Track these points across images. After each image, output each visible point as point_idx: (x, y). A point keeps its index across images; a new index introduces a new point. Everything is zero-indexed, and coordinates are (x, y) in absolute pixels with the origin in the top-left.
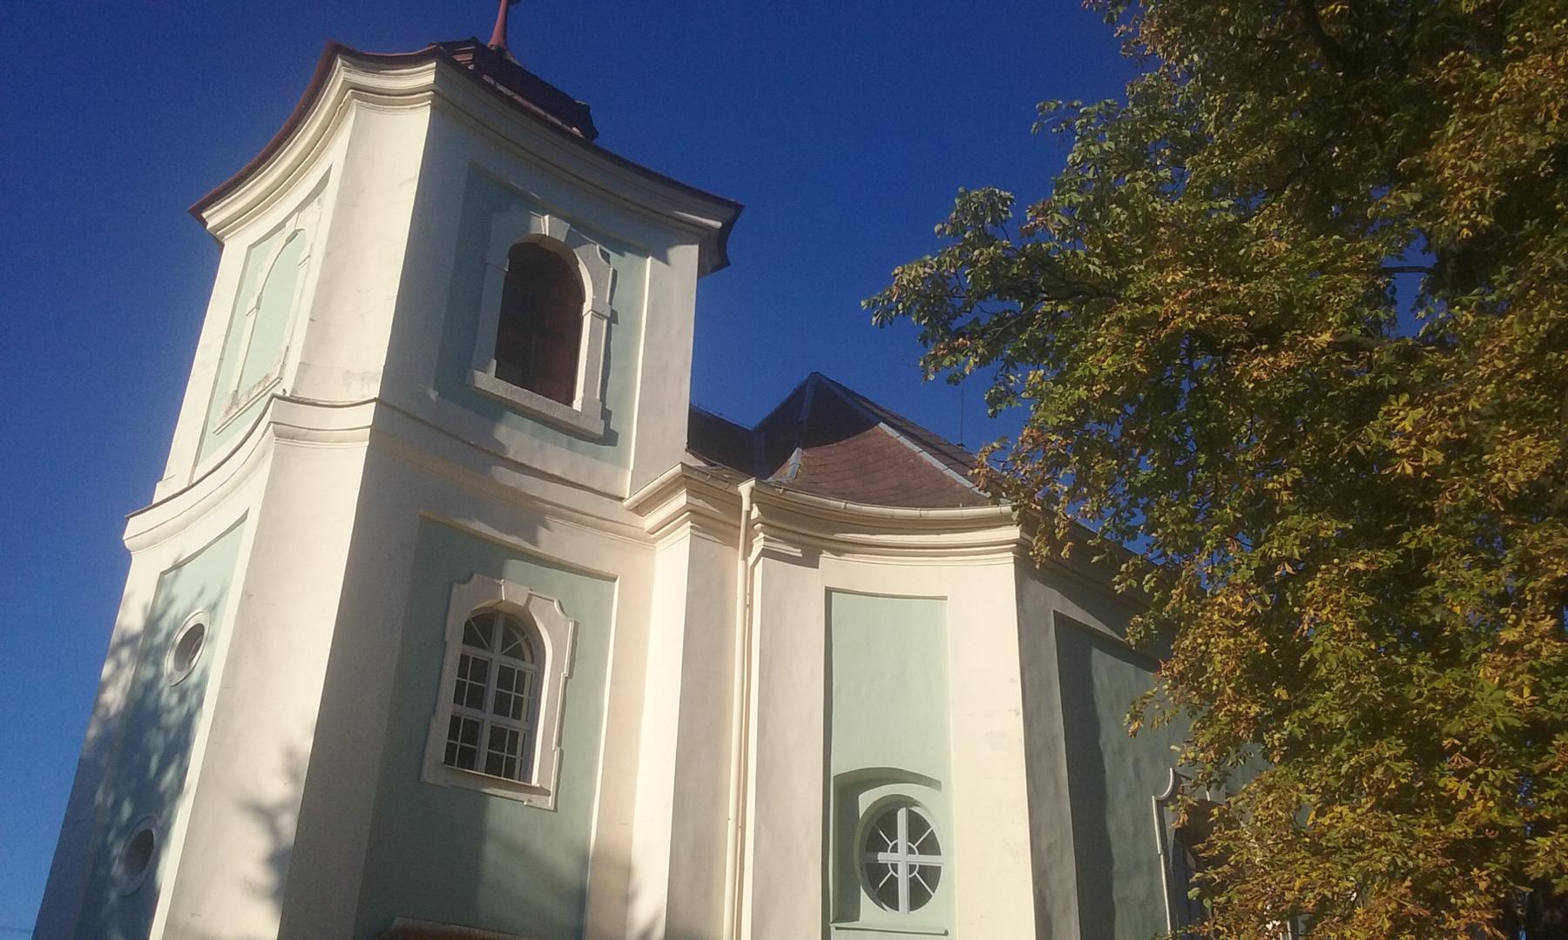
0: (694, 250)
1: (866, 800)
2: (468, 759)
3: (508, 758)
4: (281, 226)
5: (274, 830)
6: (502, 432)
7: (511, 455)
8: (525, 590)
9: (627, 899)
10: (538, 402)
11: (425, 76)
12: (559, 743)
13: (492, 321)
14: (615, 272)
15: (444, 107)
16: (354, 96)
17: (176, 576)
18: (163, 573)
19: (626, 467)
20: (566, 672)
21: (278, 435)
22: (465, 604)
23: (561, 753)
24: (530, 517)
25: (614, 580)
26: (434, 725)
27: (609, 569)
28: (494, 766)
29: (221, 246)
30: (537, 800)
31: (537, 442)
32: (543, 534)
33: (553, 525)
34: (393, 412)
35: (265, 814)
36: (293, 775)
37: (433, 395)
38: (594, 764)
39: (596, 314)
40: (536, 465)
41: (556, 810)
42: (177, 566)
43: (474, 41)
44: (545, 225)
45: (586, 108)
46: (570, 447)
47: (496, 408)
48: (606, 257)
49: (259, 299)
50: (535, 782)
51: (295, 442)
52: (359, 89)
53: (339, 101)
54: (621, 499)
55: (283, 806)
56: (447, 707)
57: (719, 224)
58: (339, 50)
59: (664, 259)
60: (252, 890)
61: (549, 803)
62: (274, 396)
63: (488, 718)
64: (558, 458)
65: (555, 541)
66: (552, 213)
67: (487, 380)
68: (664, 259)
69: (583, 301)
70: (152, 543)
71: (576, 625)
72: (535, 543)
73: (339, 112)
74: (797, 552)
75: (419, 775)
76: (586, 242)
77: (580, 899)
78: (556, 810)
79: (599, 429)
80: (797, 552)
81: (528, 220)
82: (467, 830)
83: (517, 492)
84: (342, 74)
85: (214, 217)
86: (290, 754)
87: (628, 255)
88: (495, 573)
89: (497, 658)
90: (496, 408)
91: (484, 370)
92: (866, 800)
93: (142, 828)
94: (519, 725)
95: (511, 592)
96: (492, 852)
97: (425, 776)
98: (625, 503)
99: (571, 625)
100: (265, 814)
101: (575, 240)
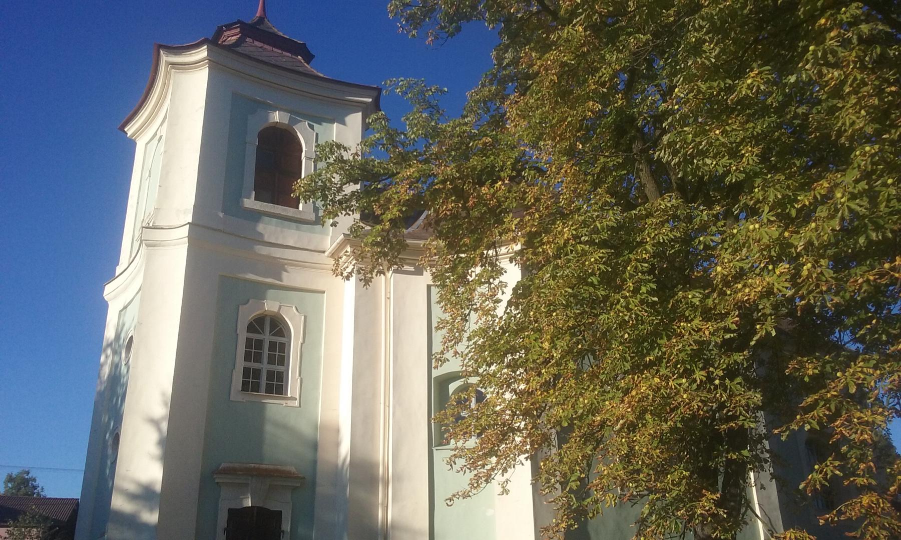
0: (359, 116)
2: (256, 388)
3: (277, 385)
4: (155, 134)
5: (159, 430)
6: (261, 227)
7: (266, 239)
8: (277, 304)
9: (338, 444)
11: (202, 53)
12: (300, 375)
13: (256, 170)
14: (317, 134)
15: (215, 65)
18: (121, 311)
19: (328, 235)
20: (301, 340)
21: (146, 245)
22: (247, 314)
24: (277, 268)
27: (320, 288)
28: (269, 390)
30: (290, 403)
31: (279, 229)
32: (285, 274)
33: (289, 270)
34: (201, 230)
35: (155, 423)
36: (166, 404)
37: (221, 215)
40: (280, 242)
42: (125, 308)
43: (239, 22)
44: (277, 117)
46: (298, 229)
48: (312, 127)
50: (289, 395)
51: (156, 248)
52: (173, 64)
54: (324, 252)
55: (163, 418)
56: (241, 364)
58: (161, 46)
61: (297, 403)
63: (265, 367)
64: (291, 236)
65: (291, 278)
66: (280, 110)
67: (250, 203)
70: (115, 297)
71: (305, 317)
72: (281, 281)
73: (168, 75)
74: (412, 269)
76: (300, 121)
77: (315, 446)
79: (312, 217)
82: (256, 421)
85: (130, 130)
86: (163, 394)
87: (324, 124)
89: (267, 337)
90: (256, 216)
91: (249, 198)
92: (453, 387)
94: (281, 368)
95: (270, 306)
96: (269, 428)
97: (232, 399)
98: (326, 254)
99: (303, 318)
100: (155, 423)
101: (293, 122)
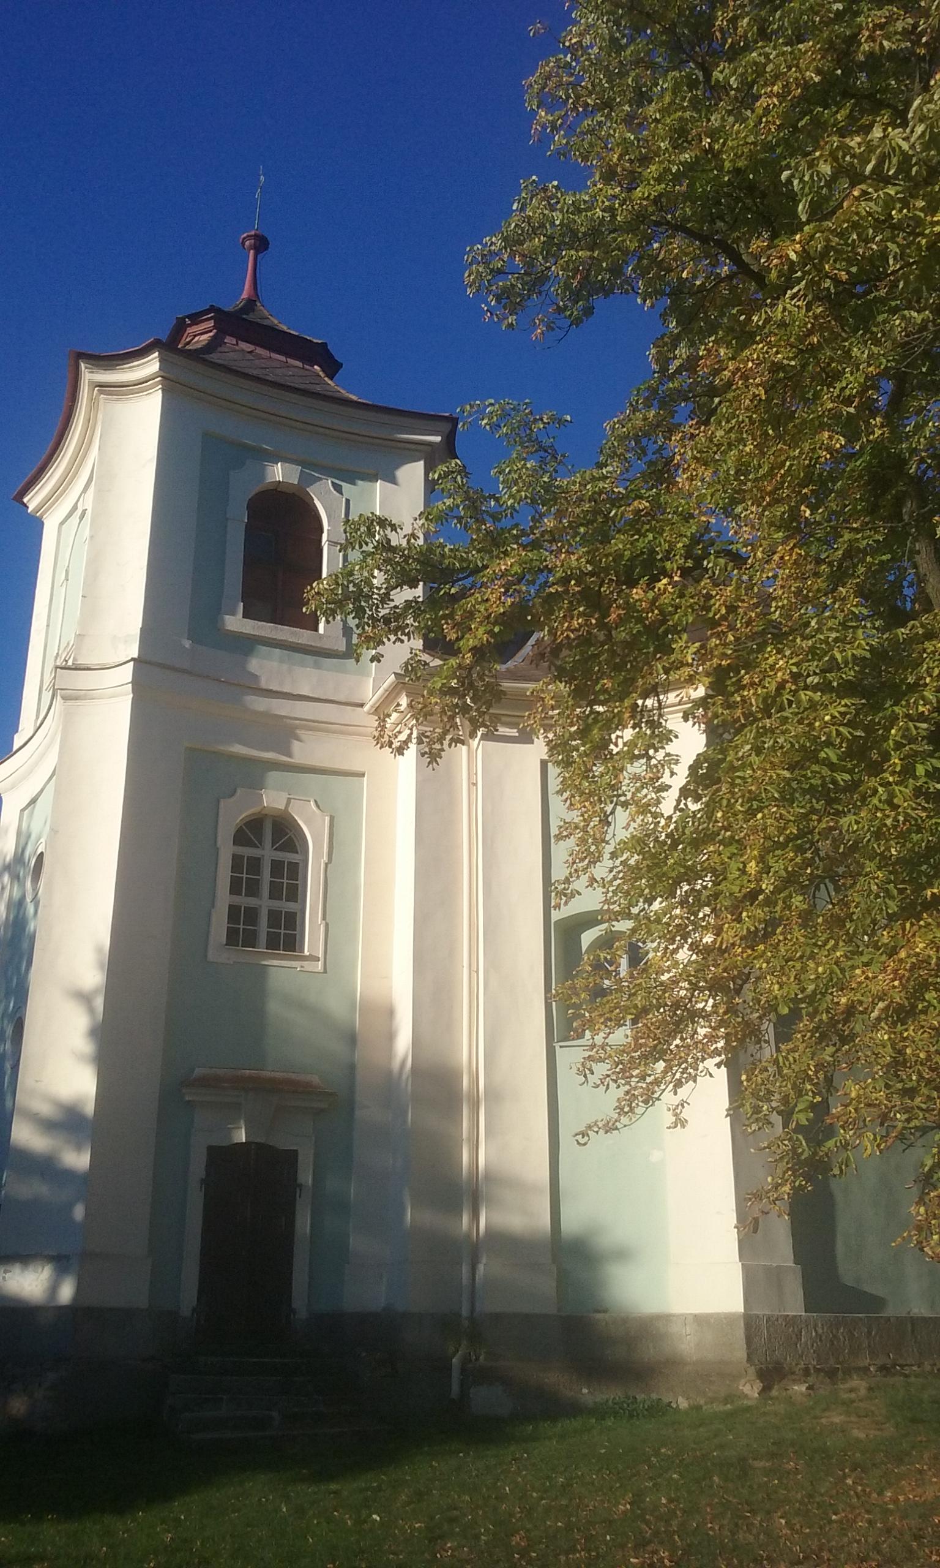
0: (420, 465)
1: (588, 938)
2: (250, 940)
3: (286, 935)
4: (75, 508)
5: (91, 1010)
6: (254, 665)
7: (264, 685)
8: (285, 795)
9: (390, 1036)
10: (284, 633)
11: (151, 365)
12: (324, 918)
13: (244, 562)
14: (348, 501)
15: (171, 385)
16: (101, 392)
17: (32, 812)
18: (23, 810)
19: (369, 675)
20: (325, 858)
21: (64, 698)
22: (233, 814)
23: (327, 925)
24: (283, 733)
25: (363, 775)
26: (214, 919)
27: (357, 767)
28: (273, 943)
29: (43, 524)
30: (308, 966)
31: (285, 667)
32: (296, 746)
33: (303, 737)
34: (153, 669)
35: (84, 998)
36: (101, 967)
37: (187, 644)
38: (355, 932)
39: (332, 543)
40: (286, 689)
41: (325, 972)
42: (33, 801)
43: (212, 309)
44: (278, 472)
45: (324, 345)
46: (317, 666)
47: (247, 645)
48: (338, 489)
49: (67, 572)
50: (306, 953)
51: (79, 703)
52: (101, 385)
53: (91, 398)
54: (362, 705)
55: (96, 991)
56: (224, 898)
57: (438, 439)
58: (81, 356)
59: (393, 480)
60: (81, 1058)
61: (320, 966)
62: (57, 667)
63: (264, 904)
64: (306, 678)
65: (308, 750)
66: (284, 460)
67: (236, 622)
68: (393, 480)
69: (322, 532)
70: (13, 787)
71: (332, 819)
72: (290, 755)
73: (93, 404)
74: (514, 732)
75: (206, 956)
76: (320, 479)
77: (352, 1039)
78: (325, 972)
79: (342, 647)
80: (514, 732)
81: (264, 468)
83: (267, 715)
84: (89, 376)
85: (33, 501)
86: (99, 950)
87: (360, 482)
88: (257, 784)
89: (268, 853)
90: (247, 645)
91: (233, 613)
92: (588, 938)
93: (18, 1015)
94: (291, 906)
95: (272, 799)
96: (274, 1007)
97: (211, 956)
98: (366, 708)
99: (327, 819)
100: (84, 998)
101: (307, 480)
